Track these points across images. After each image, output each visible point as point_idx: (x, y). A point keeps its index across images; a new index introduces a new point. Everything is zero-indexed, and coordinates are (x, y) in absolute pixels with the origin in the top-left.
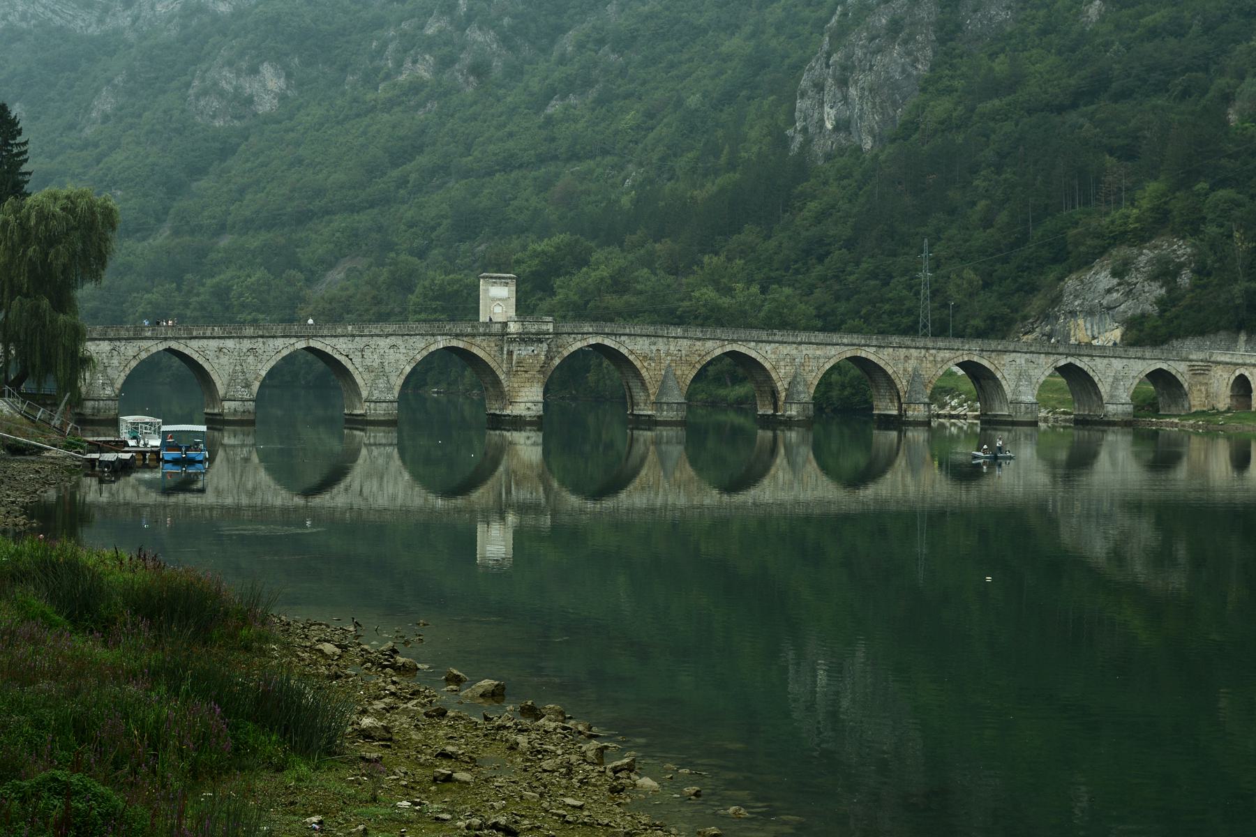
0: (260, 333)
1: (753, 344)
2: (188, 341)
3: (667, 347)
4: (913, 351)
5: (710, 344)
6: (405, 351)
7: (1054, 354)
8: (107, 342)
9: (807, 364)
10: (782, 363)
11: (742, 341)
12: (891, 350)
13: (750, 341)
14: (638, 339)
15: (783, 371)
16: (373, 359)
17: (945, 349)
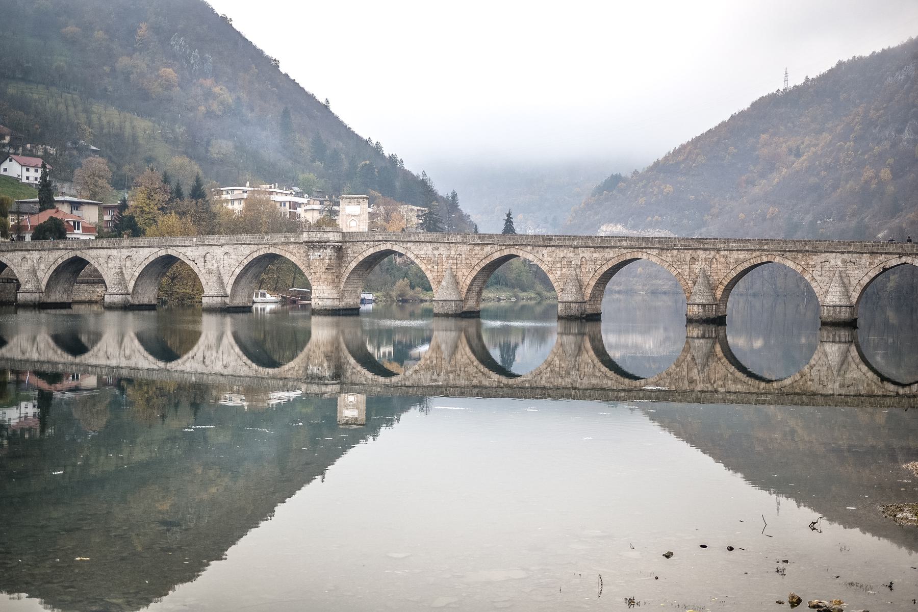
0: (133, 245)
1: (529, 248)
2: (87, 251)
3: (449, 251)
4: (701, 252)
5: (488, 249)
6: (235, 257)
7: (882, 253)
8: (36, 252)
9: (584, 266)
10: (559, 265)
11: (519, 245)
12: (675, 252)
13: (526, 246)
14: (423, 245)
15: (559, 273)
16: (212, 265)
17: (738, 250)
